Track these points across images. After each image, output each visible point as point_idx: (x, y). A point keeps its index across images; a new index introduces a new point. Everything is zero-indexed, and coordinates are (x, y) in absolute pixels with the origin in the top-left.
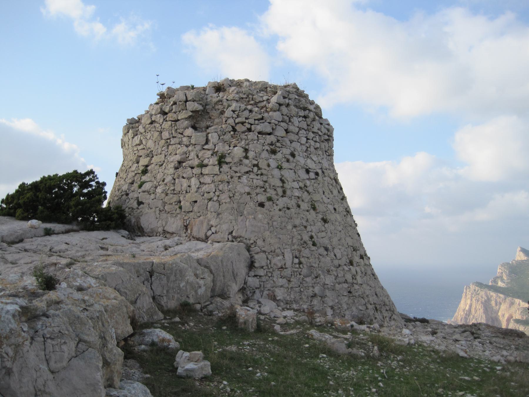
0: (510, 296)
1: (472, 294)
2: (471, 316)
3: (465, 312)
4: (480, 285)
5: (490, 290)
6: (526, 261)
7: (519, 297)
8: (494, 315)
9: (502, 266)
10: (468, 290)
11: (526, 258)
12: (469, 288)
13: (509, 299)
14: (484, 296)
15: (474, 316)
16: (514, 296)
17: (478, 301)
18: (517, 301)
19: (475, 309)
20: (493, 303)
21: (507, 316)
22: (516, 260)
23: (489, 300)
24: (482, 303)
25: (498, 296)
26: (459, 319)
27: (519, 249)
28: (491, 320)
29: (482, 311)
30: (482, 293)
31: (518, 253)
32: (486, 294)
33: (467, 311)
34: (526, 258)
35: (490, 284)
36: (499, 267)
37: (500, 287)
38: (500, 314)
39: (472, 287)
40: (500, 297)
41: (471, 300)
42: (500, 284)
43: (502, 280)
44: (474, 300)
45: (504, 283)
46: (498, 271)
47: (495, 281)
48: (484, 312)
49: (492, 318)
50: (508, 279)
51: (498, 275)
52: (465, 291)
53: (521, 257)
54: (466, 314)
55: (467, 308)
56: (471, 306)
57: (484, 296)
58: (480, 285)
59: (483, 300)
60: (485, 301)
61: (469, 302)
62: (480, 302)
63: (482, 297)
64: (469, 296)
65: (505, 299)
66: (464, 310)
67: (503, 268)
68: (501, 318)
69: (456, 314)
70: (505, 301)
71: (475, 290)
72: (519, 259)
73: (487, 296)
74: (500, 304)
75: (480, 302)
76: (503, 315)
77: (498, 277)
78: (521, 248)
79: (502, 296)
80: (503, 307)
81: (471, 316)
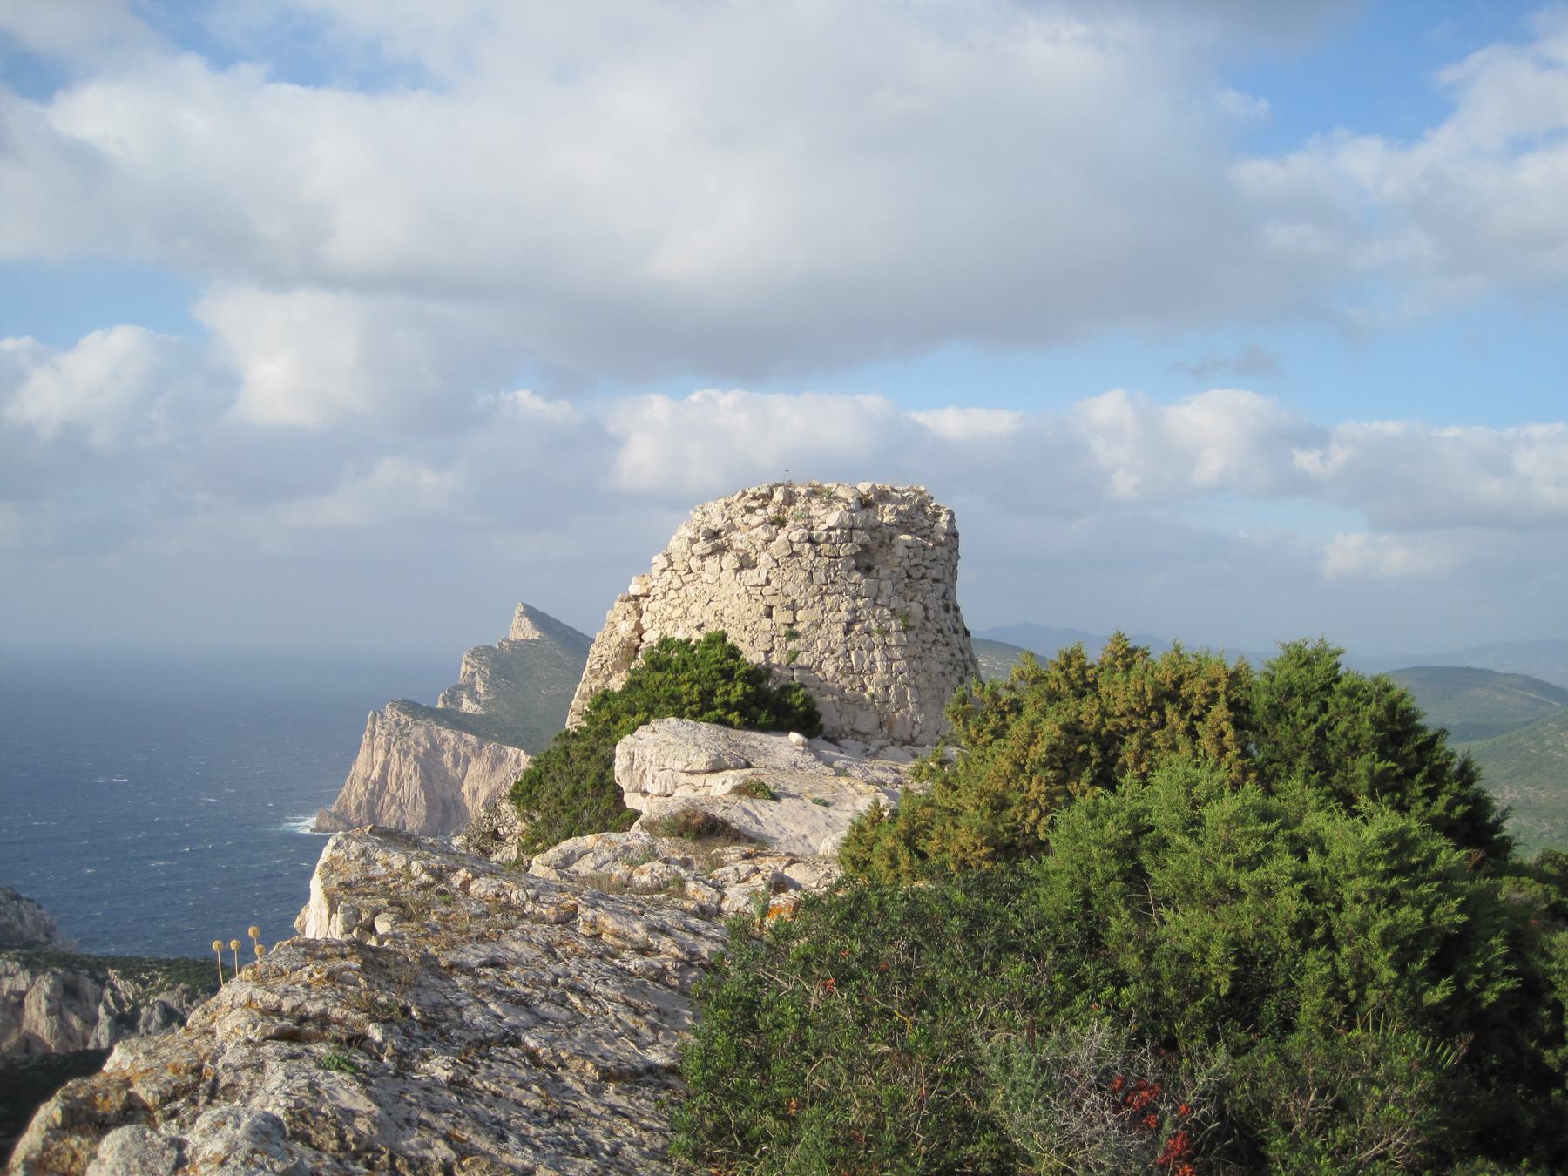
0: (496, 740)
1: (390, 734)
2: (387, 798)
3: (370, 786)
4: (413, 708)
5: (438, 724)
6: (537, 641)
7: (516, 743)
8: (448, 794)
9: (473, 655)
10: (379, 723)
11: (537, 635)
12: (382, 716)
13: (489, 748)
14: (422, 740)
15: (393, 797)
16: (503, 740)
17: (406, 754)
18: (513, 752)
19: (398, 776)
20: (448, 759)
21: (483, 794)
22: (512, 638)
23: (436, 749)
24: (416, 758)
25: (461, 739)
26: (353, 807)
27: (520, 609)
28: (440, 807)
29: (416, 781)
30: (419, 732)
31: (515, 623)
32: (428, 732)
33: (374, 782)
34: (537, 635)
35: (440, 705)
36: (466, 657)
37: (466, 715)
38: (465, 789)
39: (390, 714)
40: (466, 743)
41: (388, 752)
42: (467, 706)
43: (473, 696)
44: (394, 750)
45: (478, 702)
46: (463, 668)
47: (453, 697)
48: (422, 786)
49: (444, 802)
50: (488, 693)
51: (462, 680)
52: (369, 725)
53: (524, 631)
54: (372, 793)
55: (376, 774)
56: (385, 768)
57: (422, 740)
58: (413, 708)
59: (421, 750)
60: (426, 754)
61: (380, 757)
62: (411, 757)
63: (417, 743)
64: (380, 741)
65: (481, 748)
66: (366, 780)
67: (475, 662)
68: (468, 801)
69: (345, 791)
70: (480, 755)
71: (397, 723)
72: (520, 636)
73: (431, 739)
74: (468, 761)
75: (411, 757)
76: (475, 793)
77: (461, 688)
78: (525, 606)
79: (472, 739)
80: (475, 769)
81: (387, 798)
